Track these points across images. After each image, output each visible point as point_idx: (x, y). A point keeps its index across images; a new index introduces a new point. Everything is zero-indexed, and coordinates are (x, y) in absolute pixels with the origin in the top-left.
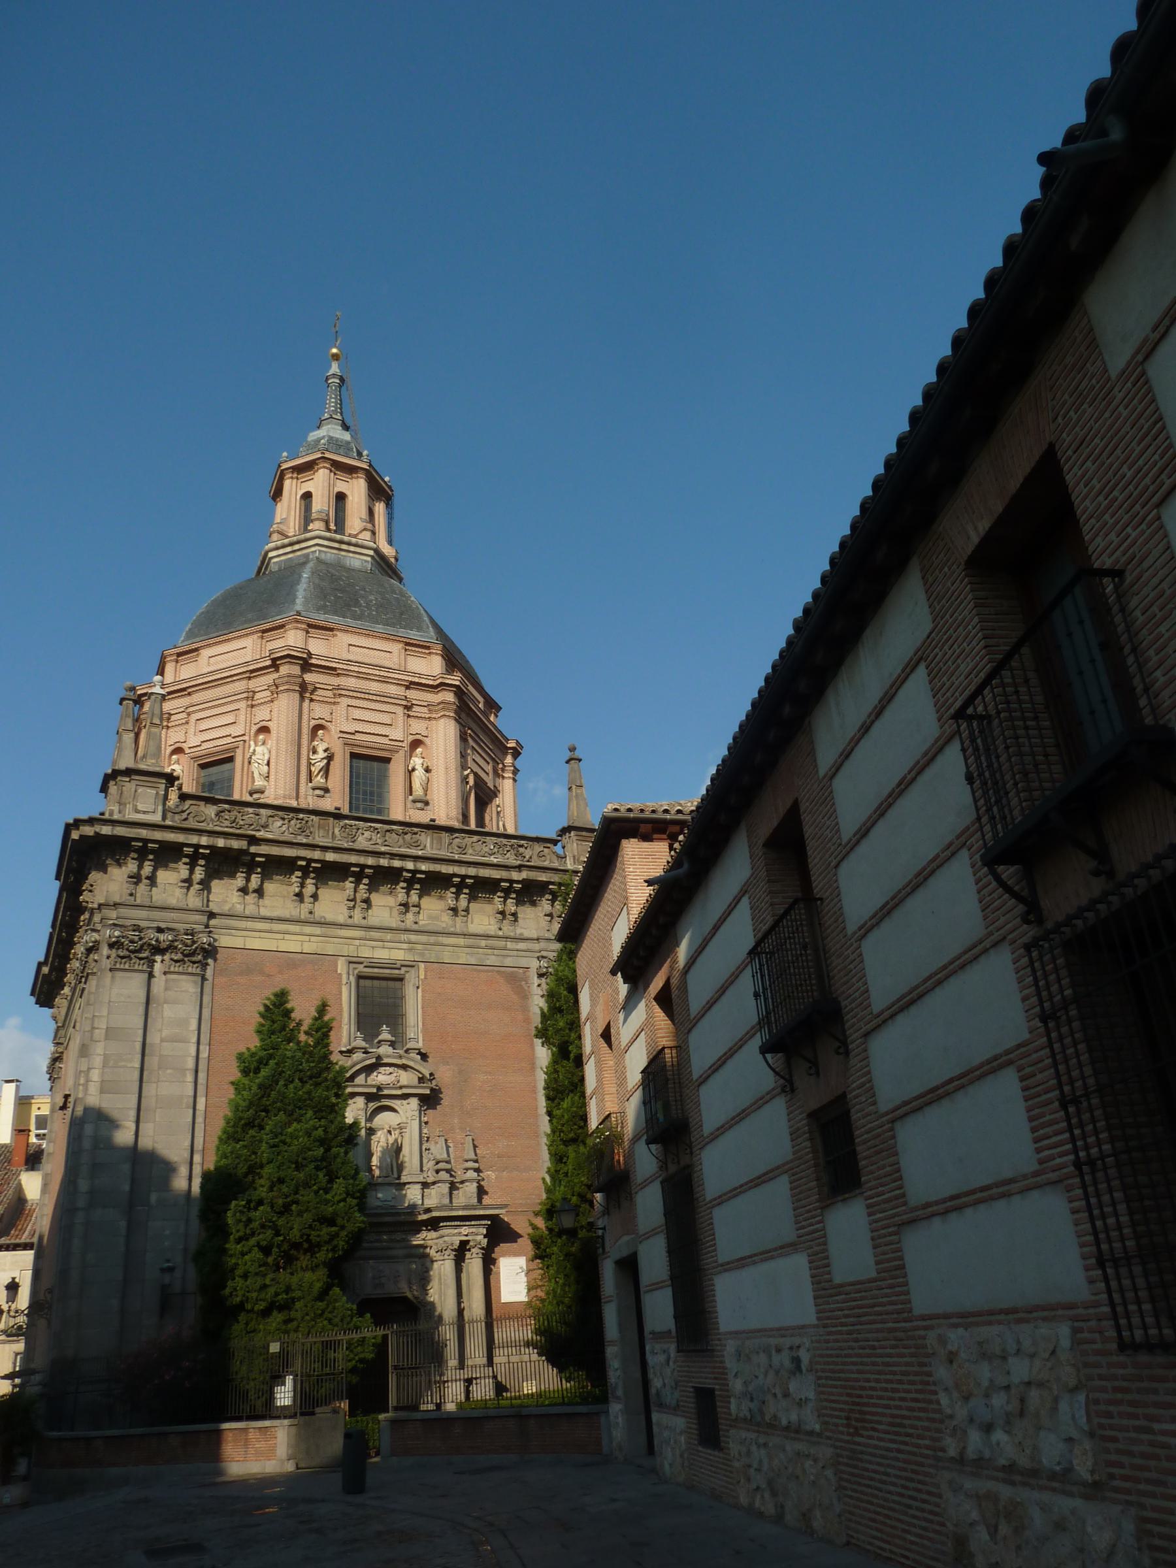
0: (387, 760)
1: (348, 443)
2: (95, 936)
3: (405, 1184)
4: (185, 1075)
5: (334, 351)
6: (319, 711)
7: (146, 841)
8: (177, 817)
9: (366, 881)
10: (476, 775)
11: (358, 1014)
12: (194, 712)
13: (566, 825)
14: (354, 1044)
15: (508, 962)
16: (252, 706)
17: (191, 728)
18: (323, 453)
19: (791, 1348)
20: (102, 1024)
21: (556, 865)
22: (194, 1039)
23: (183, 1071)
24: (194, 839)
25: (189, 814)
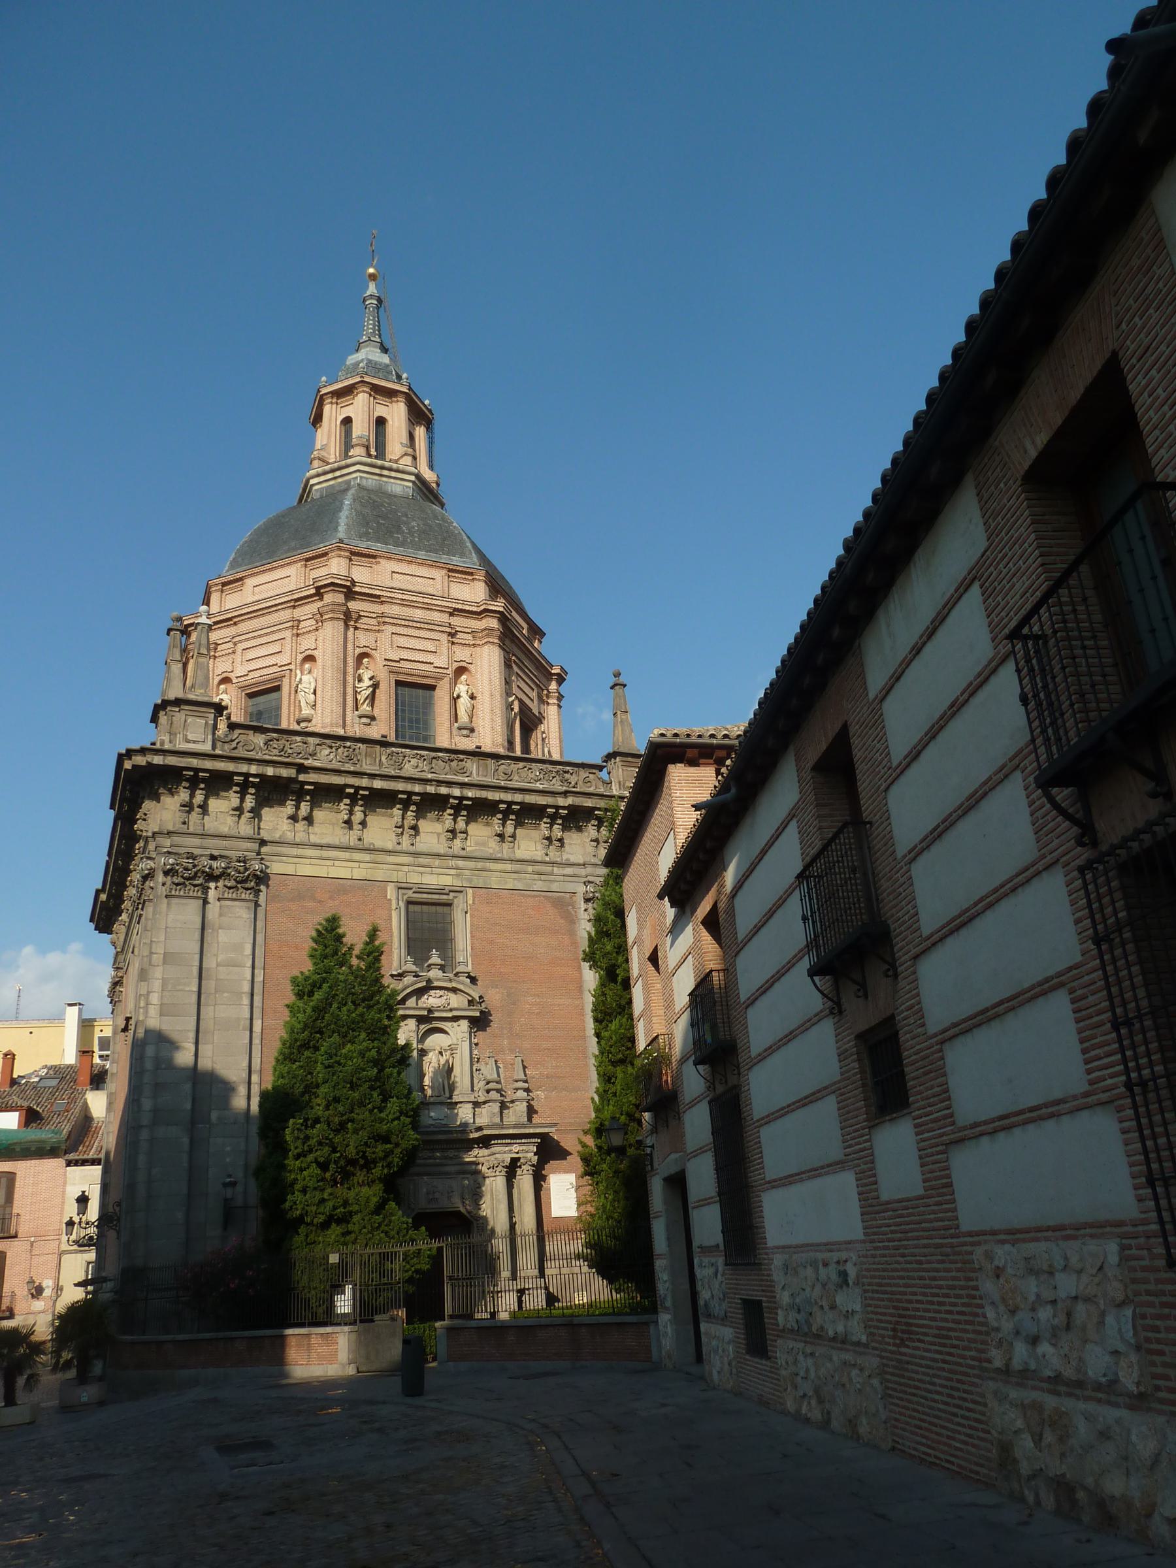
0: (433, 688)
1: (387, 366)
2: (151, 864)
3: (456, 1103)
4: (241, 998)
5: (371, 270)
6: (364, 639)
7: (197, 770)
8: (226, 746)
9: (413, 808)
10: (521, 701)
11: (408, 939)
12: (241, 641)
13: (611, 751)
14: (404, 968)
16: (298, 635)
17: (238, 657)
18: (362, 377)
19: (838, 1262)
20: (160, 950)
21: (601, 790)
22: (249, 964)
24: (244, 768)
25: (238, 743)
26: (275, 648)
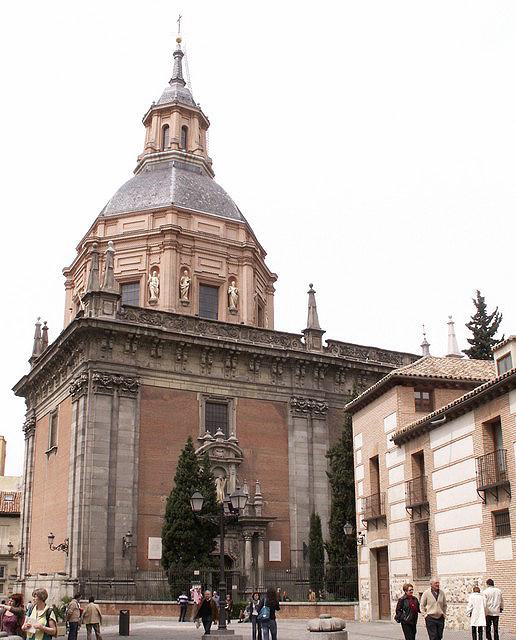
7: (111, 331)
15: (277, 398)
23: (129, 445)
24: (134, 331)
26: (137, 260)
